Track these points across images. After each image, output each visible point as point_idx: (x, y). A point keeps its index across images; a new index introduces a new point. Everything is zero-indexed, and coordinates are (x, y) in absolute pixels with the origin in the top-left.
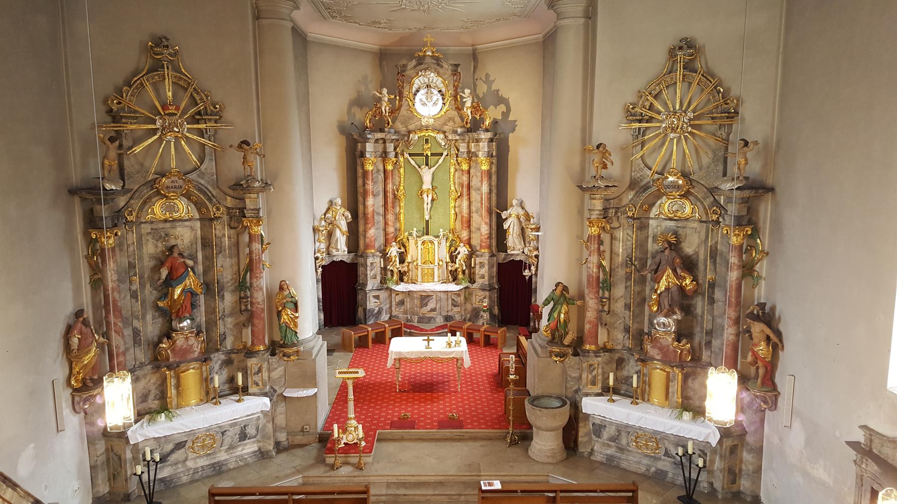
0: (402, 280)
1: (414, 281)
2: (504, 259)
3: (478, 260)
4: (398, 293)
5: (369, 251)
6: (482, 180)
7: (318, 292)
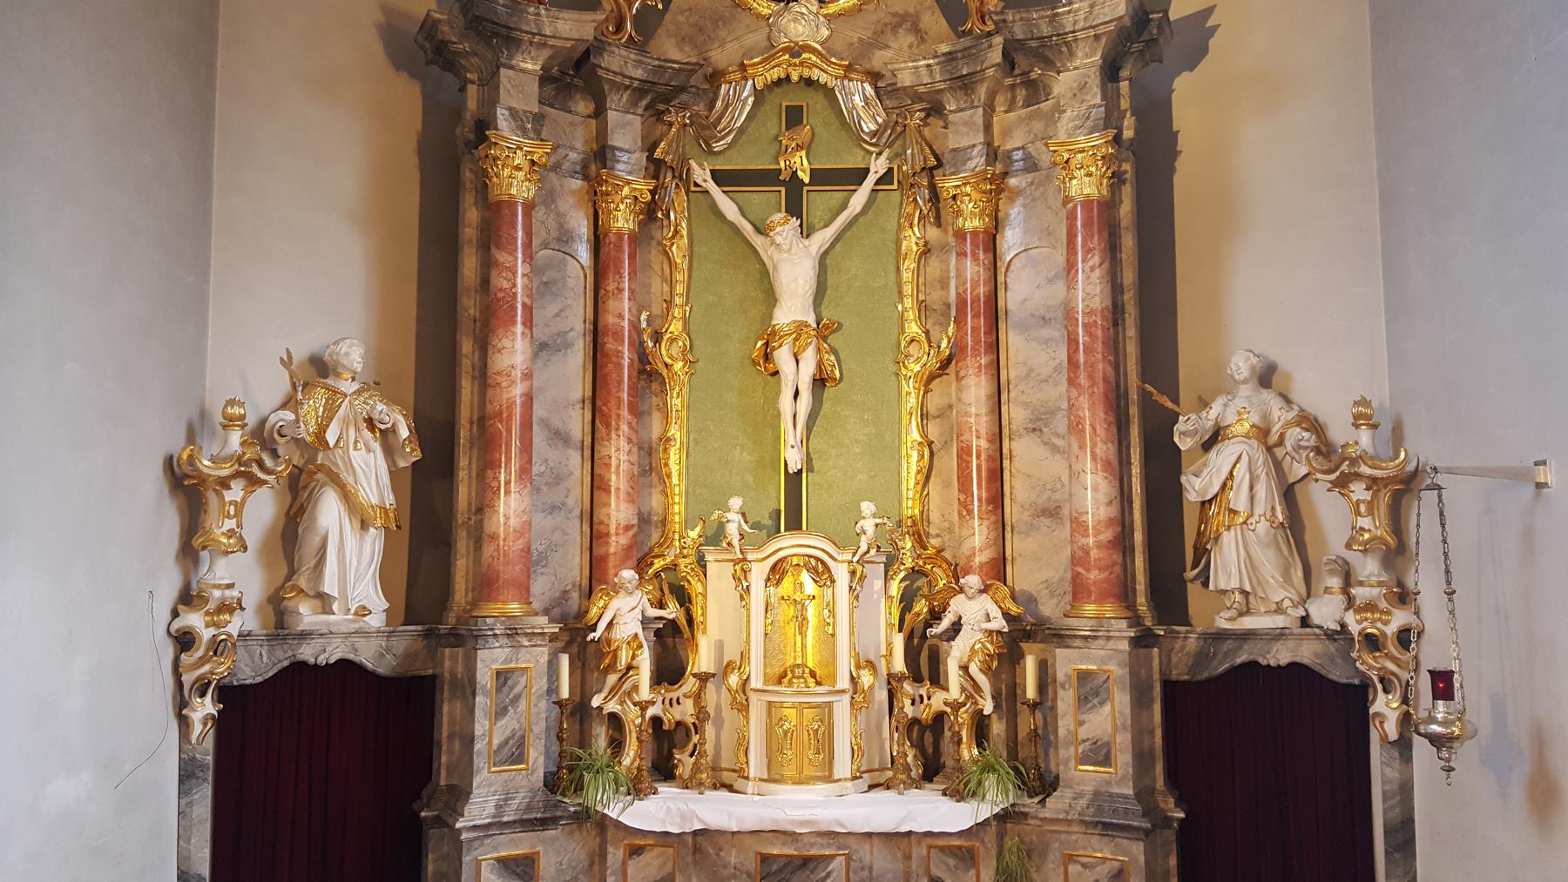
0: (664, 770)
1: (727, 777)
2: (1201, 657)
3: (1067, 662)
4: (638, 843)
5: (494, 609)
6: (1071, 266)
7: (183, 834)
